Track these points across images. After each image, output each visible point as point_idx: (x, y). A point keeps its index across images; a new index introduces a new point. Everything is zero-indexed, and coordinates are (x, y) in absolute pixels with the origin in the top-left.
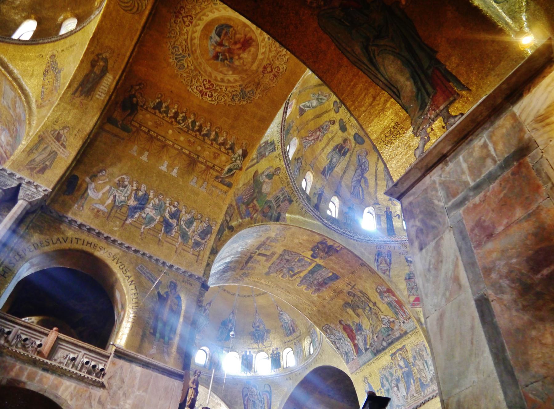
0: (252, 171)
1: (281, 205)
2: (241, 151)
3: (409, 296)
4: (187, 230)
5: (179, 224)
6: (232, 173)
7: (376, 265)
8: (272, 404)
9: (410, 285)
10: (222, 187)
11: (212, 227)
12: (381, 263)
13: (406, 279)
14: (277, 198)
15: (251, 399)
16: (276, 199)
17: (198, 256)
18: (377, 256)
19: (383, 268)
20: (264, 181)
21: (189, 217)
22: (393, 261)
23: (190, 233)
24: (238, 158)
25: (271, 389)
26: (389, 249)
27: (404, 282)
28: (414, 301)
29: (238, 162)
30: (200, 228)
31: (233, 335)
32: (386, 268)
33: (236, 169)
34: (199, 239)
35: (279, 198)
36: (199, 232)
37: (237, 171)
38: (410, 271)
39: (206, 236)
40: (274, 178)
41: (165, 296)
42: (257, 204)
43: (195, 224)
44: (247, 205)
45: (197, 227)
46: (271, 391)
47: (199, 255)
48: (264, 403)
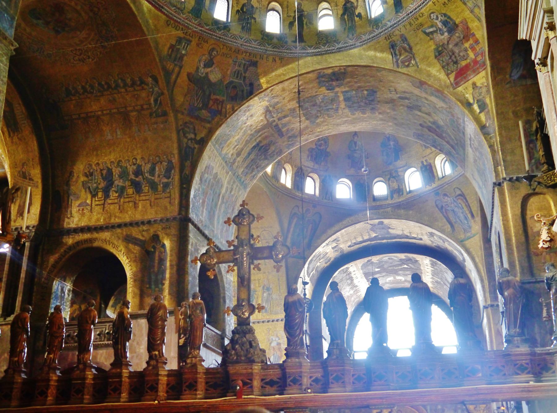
0: (184, 77)
1: (247, 75)
2: (151, 79)
3: (448, 75)
4: (153, 178)
5: (145, 177)
6: (159, 102)
7: (395, 60)
8: (471, 205)
9: (443, 62)
10: (160, 119)
11: (171, 161)
12: (400, 55)
13: (436, 57)
14: (236, 73)
15: (449, 208)
16: (236, 76)
17: (170, 197)
18: (392, 50)
19: (406, 58)
20: (207, 74)
21: (149, 166)
22: (412, 44)
23: (156, 180)
24: (154, 86)
25: (461, 191)
26: (400, 33)
27: (436, 61)
28: (456, 78)
29: (156, 89)
30: (162, 170)
31: (365, 171)
32: (409, 57)
33: (159, 96)
34: (165, 180)
35: (239, 71)
36: (163, 173)
37: (162, 97)
38: (436, 45)
39: (170, 174)
40: (215, 62)
41: (153, 250)
42: (218, 97)
43: (157, 169)
44: (205, 106)
45: (160, 169)
46: (463, 193)
47: (170, 195)
48: (463, 208)
